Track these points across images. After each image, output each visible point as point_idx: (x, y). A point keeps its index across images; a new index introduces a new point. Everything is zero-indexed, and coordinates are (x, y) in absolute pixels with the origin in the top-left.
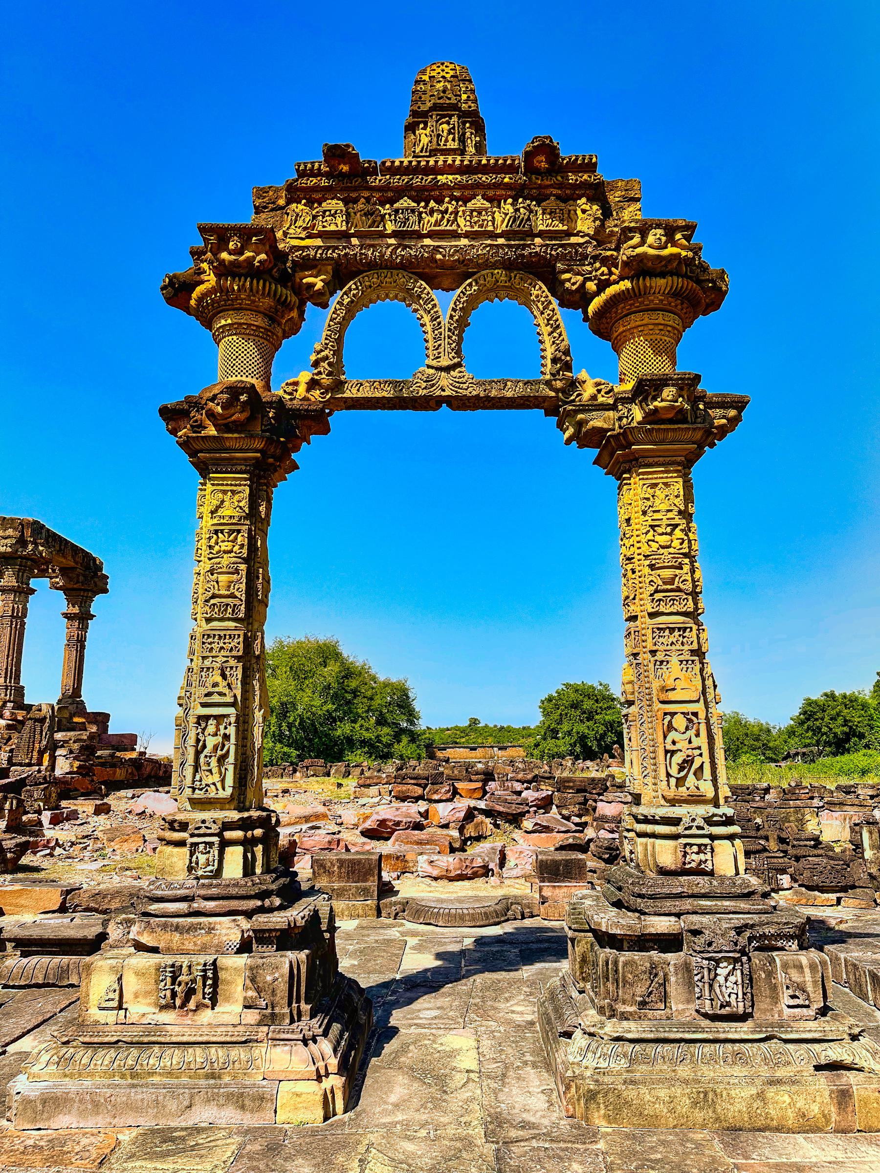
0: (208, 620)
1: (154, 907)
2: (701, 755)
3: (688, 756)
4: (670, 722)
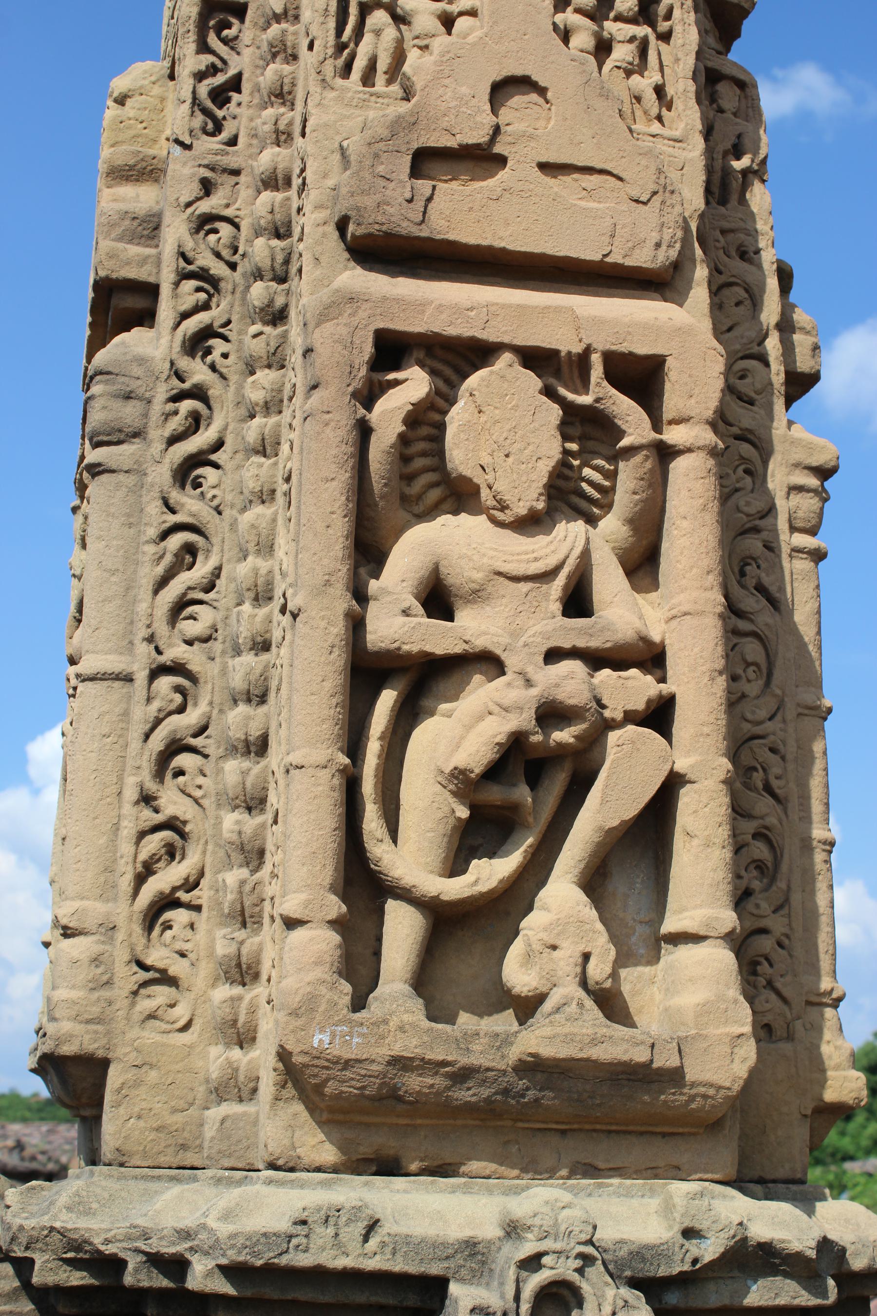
2: (659, 716)
3: (551, 714)
4: (425, 425)
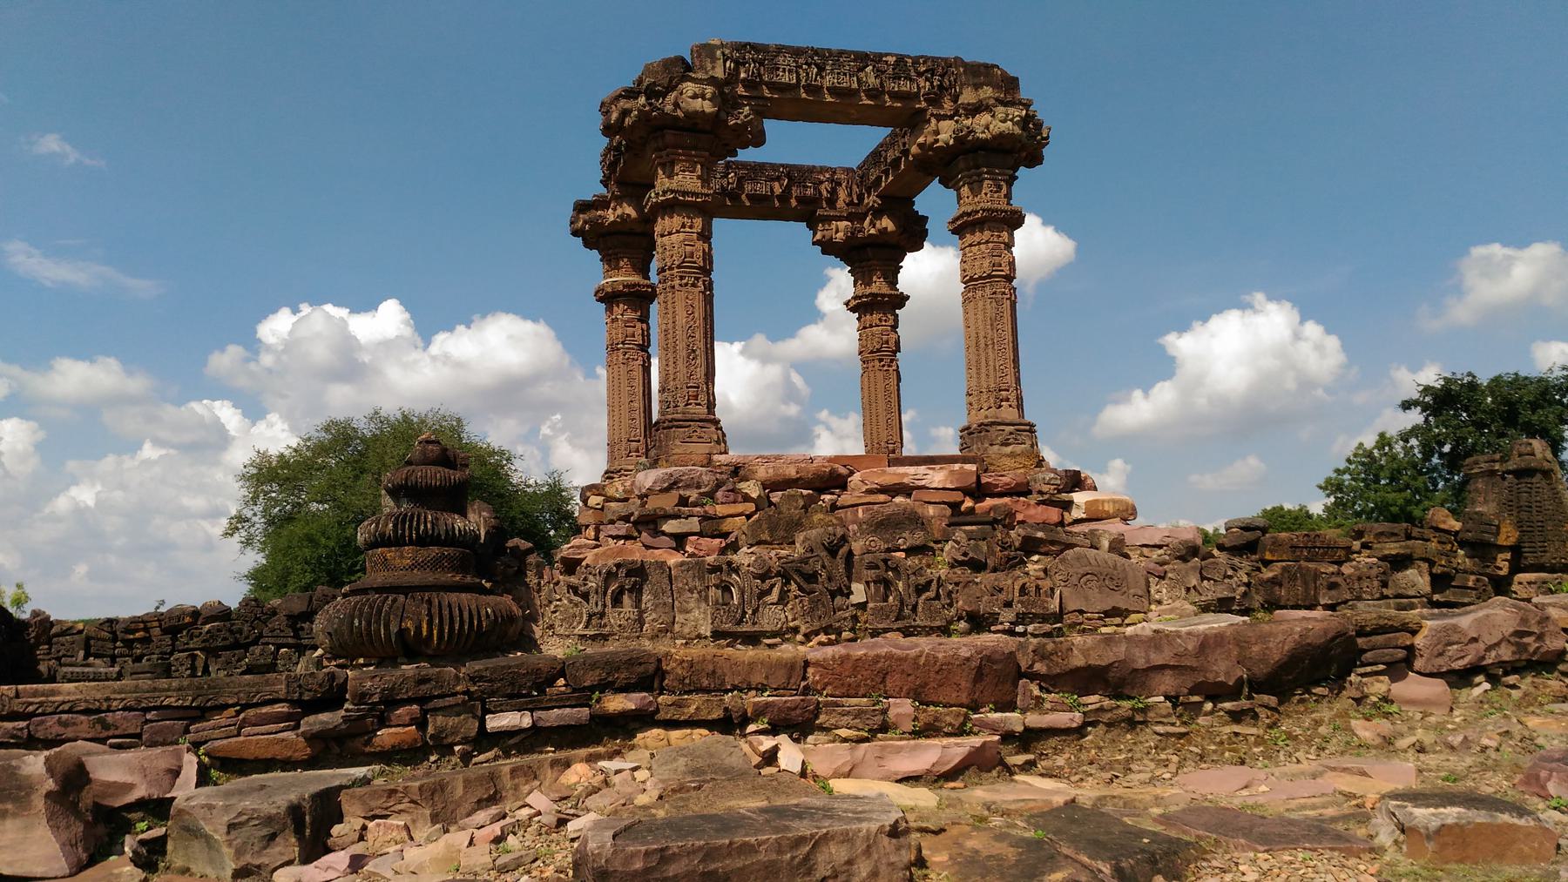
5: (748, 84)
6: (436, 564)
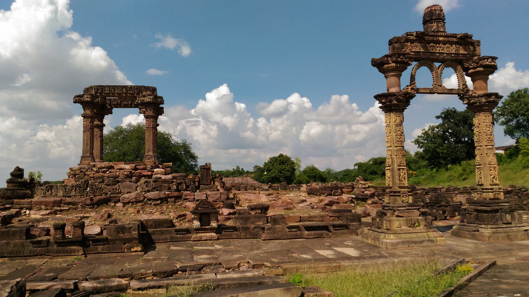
0: (396, 147)
1: (399, 208)
5: (100, 93)
6: (15, 186)
